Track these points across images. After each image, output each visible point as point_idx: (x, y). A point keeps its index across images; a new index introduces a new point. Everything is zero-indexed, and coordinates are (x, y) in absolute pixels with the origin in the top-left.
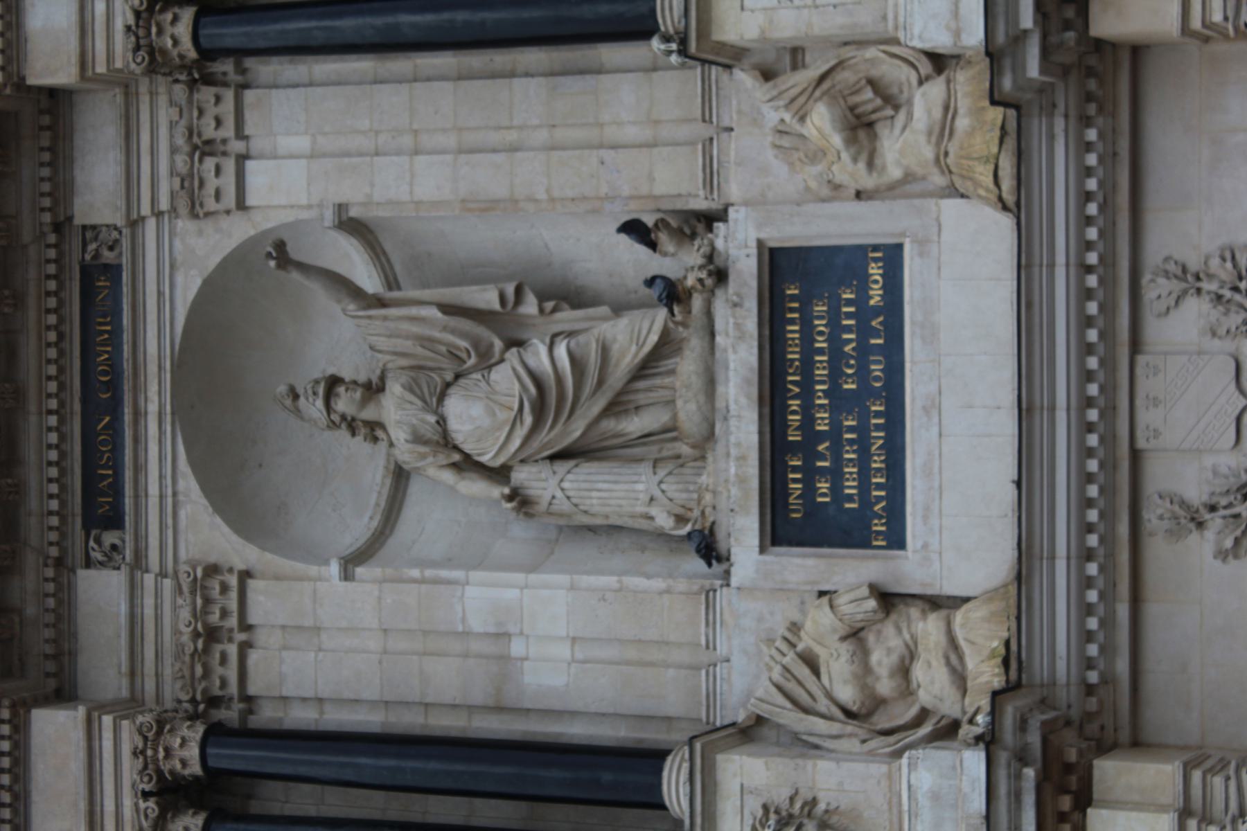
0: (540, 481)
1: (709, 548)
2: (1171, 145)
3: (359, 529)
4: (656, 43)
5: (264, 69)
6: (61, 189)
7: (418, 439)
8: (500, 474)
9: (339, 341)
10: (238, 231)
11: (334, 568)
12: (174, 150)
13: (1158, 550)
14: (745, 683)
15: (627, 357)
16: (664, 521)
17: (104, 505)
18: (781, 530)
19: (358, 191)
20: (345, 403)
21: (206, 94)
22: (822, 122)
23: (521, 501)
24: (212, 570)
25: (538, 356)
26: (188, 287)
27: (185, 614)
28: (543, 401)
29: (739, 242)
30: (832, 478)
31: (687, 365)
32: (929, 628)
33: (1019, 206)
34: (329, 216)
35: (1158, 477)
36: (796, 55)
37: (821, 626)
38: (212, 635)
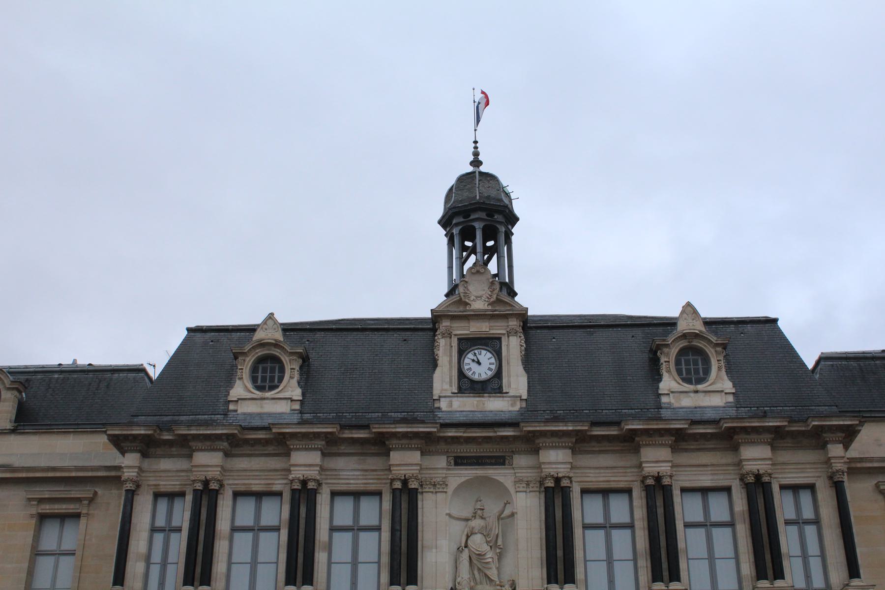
0: (465, 555)
3: (455, 513)
4: (546, 586)
5: (543, 496)
6: (519, 452)
7: (473, 528)
8: (466, 546)
10: (512, 490)
11: (448, 512)
12: (527, 477)
15: (488, 573)
16: (458, 580)
17: (459, 461)
19: (519, 516)
20: (479, 512)
21: (538, 485)
24: (447, 485)
26: (501, 479)
27: (438, 480)
28: (480, 556)
34: (515, 511)
38: (435, 485)
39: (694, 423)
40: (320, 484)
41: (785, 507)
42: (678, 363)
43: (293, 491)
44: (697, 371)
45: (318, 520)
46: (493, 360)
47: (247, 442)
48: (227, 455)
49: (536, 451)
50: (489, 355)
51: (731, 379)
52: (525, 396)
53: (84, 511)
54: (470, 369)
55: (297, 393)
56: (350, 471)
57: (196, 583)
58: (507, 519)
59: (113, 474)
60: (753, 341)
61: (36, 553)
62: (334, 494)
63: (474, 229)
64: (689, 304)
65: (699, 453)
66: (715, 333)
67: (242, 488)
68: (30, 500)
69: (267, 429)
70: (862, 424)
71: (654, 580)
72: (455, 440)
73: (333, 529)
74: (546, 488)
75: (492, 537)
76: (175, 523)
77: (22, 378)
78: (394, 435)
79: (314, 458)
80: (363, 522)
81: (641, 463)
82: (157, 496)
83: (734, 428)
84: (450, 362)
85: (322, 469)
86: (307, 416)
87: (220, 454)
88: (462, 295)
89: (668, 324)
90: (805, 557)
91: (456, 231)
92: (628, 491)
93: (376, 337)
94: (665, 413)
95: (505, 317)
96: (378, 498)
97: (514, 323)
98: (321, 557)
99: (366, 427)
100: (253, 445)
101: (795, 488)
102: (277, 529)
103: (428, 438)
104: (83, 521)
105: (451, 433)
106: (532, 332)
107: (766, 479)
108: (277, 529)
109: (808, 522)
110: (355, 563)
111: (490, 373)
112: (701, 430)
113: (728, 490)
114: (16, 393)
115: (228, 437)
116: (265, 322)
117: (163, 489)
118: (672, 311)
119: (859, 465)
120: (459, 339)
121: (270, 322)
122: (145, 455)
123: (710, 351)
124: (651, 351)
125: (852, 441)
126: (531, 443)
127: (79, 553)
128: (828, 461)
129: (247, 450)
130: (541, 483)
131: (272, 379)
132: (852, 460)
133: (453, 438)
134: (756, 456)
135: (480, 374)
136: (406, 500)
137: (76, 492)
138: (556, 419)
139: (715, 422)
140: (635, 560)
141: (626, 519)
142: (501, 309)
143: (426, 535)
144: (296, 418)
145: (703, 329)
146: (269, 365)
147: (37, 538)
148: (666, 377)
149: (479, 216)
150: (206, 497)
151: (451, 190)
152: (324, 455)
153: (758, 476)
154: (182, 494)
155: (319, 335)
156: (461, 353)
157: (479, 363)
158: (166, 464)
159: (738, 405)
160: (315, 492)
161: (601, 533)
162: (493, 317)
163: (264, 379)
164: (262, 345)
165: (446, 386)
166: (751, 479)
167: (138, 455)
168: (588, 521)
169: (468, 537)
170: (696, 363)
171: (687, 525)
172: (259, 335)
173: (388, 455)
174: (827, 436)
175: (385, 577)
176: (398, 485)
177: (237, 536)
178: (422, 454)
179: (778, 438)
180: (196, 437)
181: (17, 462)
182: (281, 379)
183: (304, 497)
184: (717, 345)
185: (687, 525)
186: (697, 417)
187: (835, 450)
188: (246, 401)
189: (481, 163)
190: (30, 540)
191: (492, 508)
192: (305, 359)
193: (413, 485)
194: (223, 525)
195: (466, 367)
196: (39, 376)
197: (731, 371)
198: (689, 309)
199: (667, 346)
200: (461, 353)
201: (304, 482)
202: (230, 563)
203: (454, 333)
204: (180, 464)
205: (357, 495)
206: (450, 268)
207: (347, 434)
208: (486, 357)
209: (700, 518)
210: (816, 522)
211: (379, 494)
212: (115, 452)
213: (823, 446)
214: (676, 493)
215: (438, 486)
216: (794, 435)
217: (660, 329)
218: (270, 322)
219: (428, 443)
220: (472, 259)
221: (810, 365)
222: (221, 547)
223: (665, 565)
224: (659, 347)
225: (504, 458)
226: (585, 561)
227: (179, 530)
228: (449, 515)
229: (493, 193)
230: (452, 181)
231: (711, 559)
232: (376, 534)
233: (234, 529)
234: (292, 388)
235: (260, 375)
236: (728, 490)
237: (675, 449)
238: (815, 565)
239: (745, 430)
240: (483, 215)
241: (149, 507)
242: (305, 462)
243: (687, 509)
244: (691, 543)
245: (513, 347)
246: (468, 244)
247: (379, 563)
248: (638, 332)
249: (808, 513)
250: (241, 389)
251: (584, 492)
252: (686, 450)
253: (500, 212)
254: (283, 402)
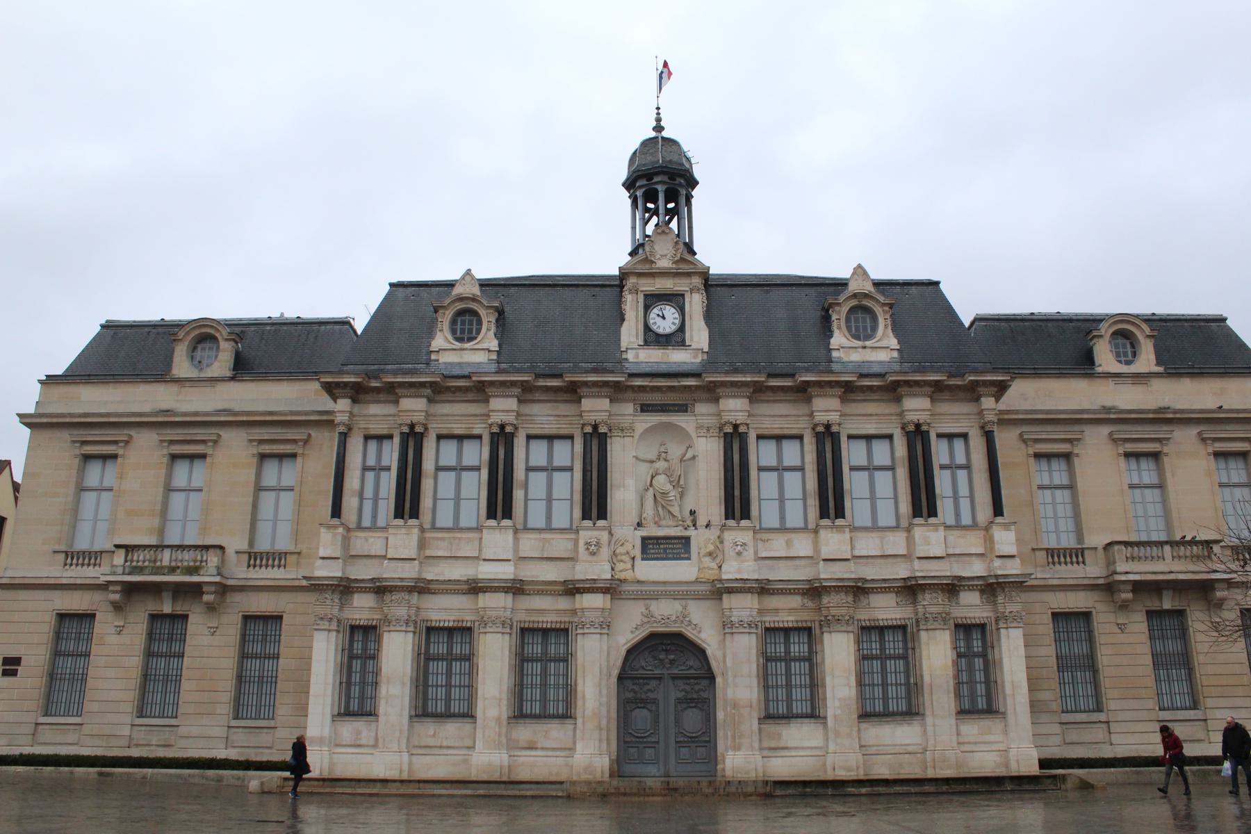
0: (650, 493)
1: (639, 525)
2: (707, 603)
3: (641, 456)
5: (722, 440)
6: (700, 401)
9: (675, 451)
10: (694, 435)
13: (642, 602)
14: (619, 532)
17: (645, 408)
18: (644, 539)
19: (700, 459)
22: (711, 548)
23: (647, 490)
25: (672, 494)
26: (683, 425)
28: (664, 494)
29: (691, 532)
30: (653, 547)
31: (671, 523)
32: (629, 566)
33: (697, 582)
35: (654, 602)
36: (722, 542)
37: (628, 547)
39: (862, 376)
40: (516, 428)
41: (940, 453)
42: (848, 320)
43: (492, 434)
44: (865, 328)
45: (515, 461)
46: (677, 315)
47: (448, 389)
48: (430, 401)
49: (716, 400)
50: (673, 310)
51: (896, 336)
52: (706, 349)
53: (300, 451)
55: (494, 344)
56: (545, 416)
57: (406, 516)
58: (688, 461)
59: (325, 418)
60: (915, 303)
61: (259, 489)
62: (530, 437)
63: (656, 191)
64: (860, 266)
65: (865, 404)
66: (883, 293)
67: (445, 432)
68: (251, 441)
69: (468, 377)
70: (1013, 379)
71: (822, 517)
72: (642, 389)
73: (529, 469)
74: (725, 434)
75: (675, 477)
76: (385, 463)
77: (237, 330)
78: (585, 384)
79: (512, 404)
80: (556, 463)
81: (812, 412)
82: (367, 438)
83: (898, 381)
84: (637, 317)
85: (518, 414)
86: (503, 366)
87: (425, 400)
89: (840, 284)
90: (956, 497)
91: (639, 193)
92: (800, 437)
93: (567, 293)
94: (835, 367)
95: (689, 275)
96: (569, 442)
97: (697, 281)
98: (518, 495)
99: (560, 376)
100: (454, 393)
101: (950, 437)
102: (478, 469)
103: (617, 386)
104: (299, 459)
105: (638, 382)
106: (712, 289)
107: (924, 428)
108: (478, 469)
109: (960, 467)
110: (549, 500)
111: (674, 328)
112: (867, 382)
113: (890, 437)
114: (233, 343)
115: (432, 384)
116: (463, 278)
117: (372, 432)
118: (843, 272)
119: (1006, 417)
121: (468, 278)
122: (355, 401)
123: (878, 310)
124: (823, 308)
125: (1002, 395)
126: (712, 392)
127: (297, 489)
128: (981, 413)
129: (449, 396)
130: (721, 429)
131: (470, 331)
132: (1002, 412)
133: (640, 387)
134: (917, 407)
136: (597, 441)
137: (291, 434)
138: (736, 371)
139: (881, 376)
140: (804, 499)
141: (798, 463)
142: (685, 268)
143: (614, 475)
144: (493, 368)
145: (872, 289)
146: (467, 318)
147: (259, 475)
148: (836, 333)
149: (661, 180)
150: (413, 439)
151: (635, 153)
152: (520, 401)
153: (918, 426)
154: (390, 437)
155: (513, 290)
156: (647, 308)
157: (663, 318)
158: (374, 409)
159: (902, 360)
160: (512, 435)
161: (775, 474)
162: (677, 275)
163: (463, 331)
164: (461, 299)
165: (633, 339)
166: (911, 428)
167: (348, 401)
168: (763, 463)
169: (653, 477)
170: (864, 320)
171: (852, 469)
172: (457, 290)
173: (580, 402)
174: (981, 390)
175: (577, 513)
176: (589, 429)
177: (441, 474)
178: (611, 401)
179: (938, 390)
180: (401, 385)
181: (237, 408)
182: (478, 332)
183: (502, 439)
184: (884, 304)
185: (852, 469)
186: (865, 371)
187: (988, 403)
188: (446, 351)
189: (663, 129)
190: (253, 477)
191: (675, 451)
192: (500, 312)
193: (602, 430)
194: (428, 465)
196: (253, 328)
197: (897, 329)
198: (860, 270)
199: (839, 304)
200: (647, 308)
201: (502, 427)
202: (435, 499)
204: (388, 409)
205: (551, 438)
206: (634, 228)
207: (541, 383)
208: (670, 312)
209: (864, 463)
210: (967, 467)
211: (571, 437)
212: (326, 397)
213: (977, 399)
214: (844, 439)
215: (625, 431)
216: (950, 388)
217: (832, 289)
218: (468, 278)
219: (617, 391)
220: (655, 220)
221: (967, 324)
222: (427, 485)
223: (831, 504)
224: (831, 305)
225: (686, 405)
226: (760, 500)
227: (388, 469)
228: (636, 458)
229: (675, 158)
230: (636, 145)
231: (873, 498)
232: (569, 474)
233: (439, 469)
234: (489, 340)
235: (459, 327)
236: (890, 437)
237: (843, 400)
238: (965, 504)
239: (907, 383)
240: (665, 178)
241: (361, 448)
242: (503, 408)
243: (853, 454)
244: (855, 484)
245: (696, 303)
246: (650, 206)
247: (571, 499)
248: (812, 292)
249: (960, 459)
250: (441, 340)
251: (759, 437)
252: (854, 401)
253: (682, 176)
254: (481, 353)
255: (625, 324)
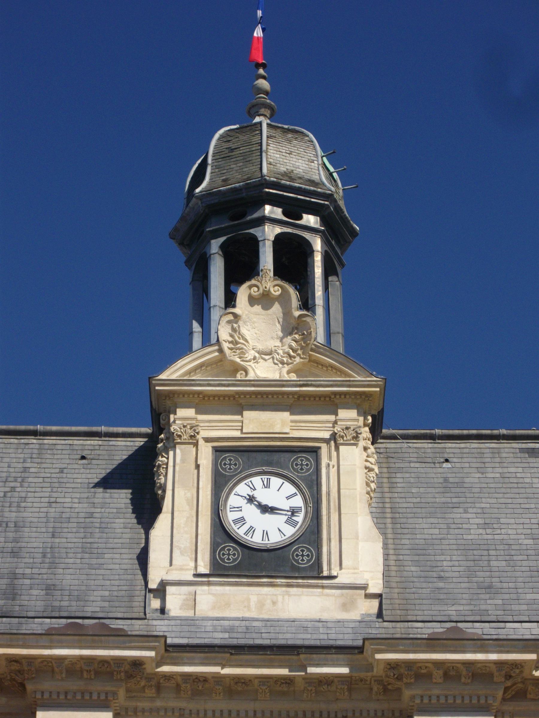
46: (298, 502)
50: (289, 488)
52: (376, 586)
54: (241, 521)
88: (226, 346)
111: (290, 531)
120: (217, 450)
135: (265, 534)
195: (231, 516)
200: (221, 484)
203: (204, 434)
208: (280, 492)
255: (162, 522)
